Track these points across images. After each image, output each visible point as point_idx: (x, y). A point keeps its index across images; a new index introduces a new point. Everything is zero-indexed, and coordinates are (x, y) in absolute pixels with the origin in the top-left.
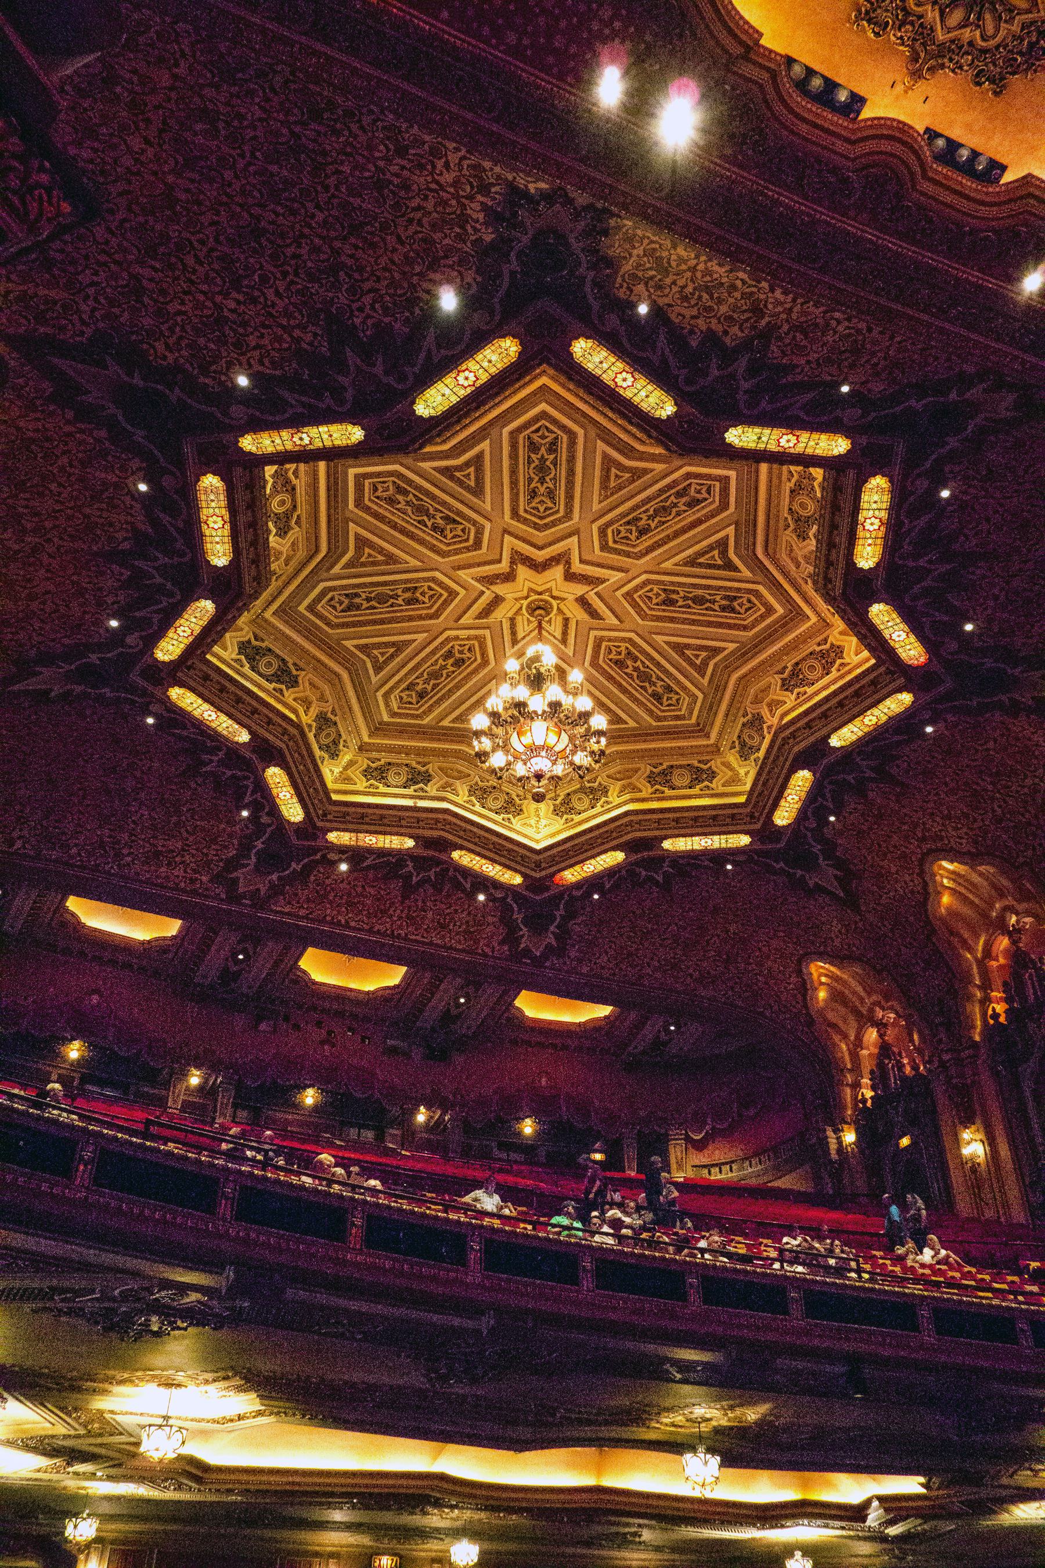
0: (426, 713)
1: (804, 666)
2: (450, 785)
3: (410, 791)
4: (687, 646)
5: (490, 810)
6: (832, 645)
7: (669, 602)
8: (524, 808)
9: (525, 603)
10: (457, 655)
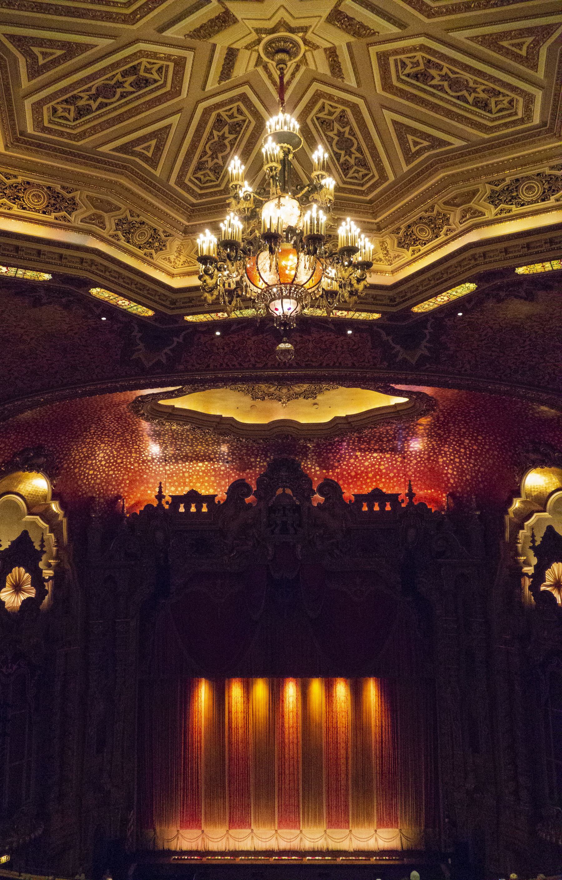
0: (82, 135)
1: (523, 187)
2: (100, 217)
3: (51, 218)
4: (414, 132)
5: (135, 245)
7: (422, 76)
8: (168, 244)
9: (266, 38)
10: (142, 73)
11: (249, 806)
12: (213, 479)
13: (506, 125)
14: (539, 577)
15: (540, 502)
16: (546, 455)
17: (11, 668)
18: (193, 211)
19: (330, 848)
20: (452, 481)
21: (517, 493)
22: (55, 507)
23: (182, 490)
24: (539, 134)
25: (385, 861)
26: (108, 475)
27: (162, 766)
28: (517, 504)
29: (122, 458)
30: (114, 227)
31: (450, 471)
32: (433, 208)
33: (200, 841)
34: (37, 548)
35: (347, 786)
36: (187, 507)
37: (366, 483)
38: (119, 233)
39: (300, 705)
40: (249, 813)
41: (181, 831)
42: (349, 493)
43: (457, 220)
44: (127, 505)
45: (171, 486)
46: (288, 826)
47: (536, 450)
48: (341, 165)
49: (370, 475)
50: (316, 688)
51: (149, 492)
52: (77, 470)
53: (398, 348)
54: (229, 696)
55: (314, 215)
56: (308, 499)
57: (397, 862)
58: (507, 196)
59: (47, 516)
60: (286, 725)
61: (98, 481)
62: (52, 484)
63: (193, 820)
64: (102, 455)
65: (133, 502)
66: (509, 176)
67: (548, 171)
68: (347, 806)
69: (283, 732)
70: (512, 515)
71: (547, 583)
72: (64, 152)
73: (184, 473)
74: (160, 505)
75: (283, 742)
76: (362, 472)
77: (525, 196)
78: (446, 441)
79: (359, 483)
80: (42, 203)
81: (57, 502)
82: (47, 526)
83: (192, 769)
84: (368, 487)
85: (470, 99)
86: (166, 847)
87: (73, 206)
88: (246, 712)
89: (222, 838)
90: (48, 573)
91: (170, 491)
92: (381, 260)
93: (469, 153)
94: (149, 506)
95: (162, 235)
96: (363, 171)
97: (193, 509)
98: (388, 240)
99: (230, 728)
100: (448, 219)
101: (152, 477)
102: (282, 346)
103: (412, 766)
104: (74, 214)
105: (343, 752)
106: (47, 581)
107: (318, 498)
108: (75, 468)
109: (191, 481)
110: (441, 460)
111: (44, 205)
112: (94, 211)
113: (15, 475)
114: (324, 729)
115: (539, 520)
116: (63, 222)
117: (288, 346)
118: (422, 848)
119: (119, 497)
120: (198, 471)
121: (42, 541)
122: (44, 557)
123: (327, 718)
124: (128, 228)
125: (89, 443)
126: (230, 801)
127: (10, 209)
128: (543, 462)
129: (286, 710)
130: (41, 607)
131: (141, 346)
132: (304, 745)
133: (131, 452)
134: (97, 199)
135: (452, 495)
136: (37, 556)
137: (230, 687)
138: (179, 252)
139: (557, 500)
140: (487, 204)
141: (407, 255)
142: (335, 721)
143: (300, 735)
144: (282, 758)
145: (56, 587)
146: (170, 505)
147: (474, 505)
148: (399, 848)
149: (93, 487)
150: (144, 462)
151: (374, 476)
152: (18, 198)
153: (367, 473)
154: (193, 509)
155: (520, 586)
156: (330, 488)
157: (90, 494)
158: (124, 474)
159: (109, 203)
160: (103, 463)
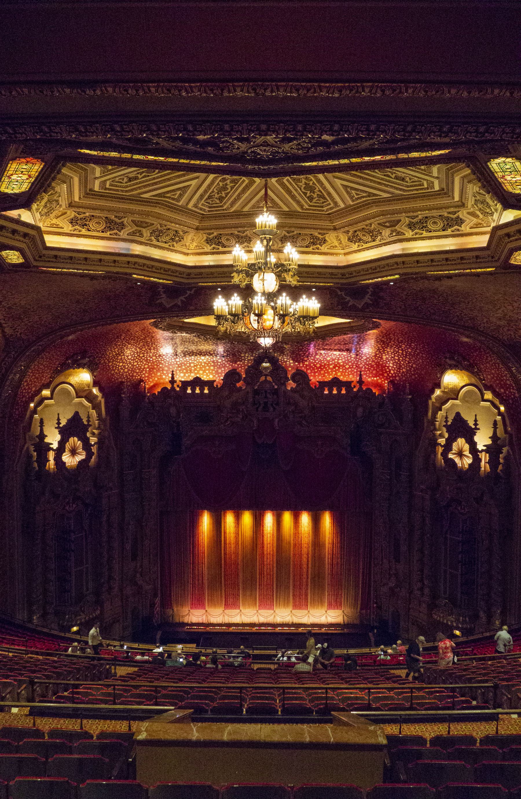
3: (107, 234)
5: (162, 242)
6: (458, 217)
11: (238, 595)
12: (212, 368)
13: (417, 190)
14: (448, 447)
15: (453, 393)
16: (458, 362)
18: (203, 218)
19: (294, 622)
20: (392, 372)
21: (438, 385)
22: (95, 391)
23: (189, 376)
24: (439, 194)
25: (332, 630)
26: (133, 365)
27: (175, 566)
28: (438, 392)
29: (143, 353)
30: (149, 235)
31: (391, 365)
32: (371, 224)
33: (204, 617)
34: (86, 423)
35: (307, 582)
36: (193, 390)
37: (328, 373)
38: (153, 238)
39: (275, 529)
40: (238, 599)
41: (191, 611)
42: (314, 379)
43: (387, 234)
44: (147, 386)
45: (180, 373)
46: (265, 608)
47: (452, 358)
48: (308, 198)
49: (331, 367)
50: (287, 517)
51: (164, 377)
52: (110, 364)
53: (348, 298)
54: (225, 522)
55: (284, 302)
56: (284, 384)
57: (339, 632)
58: (420, 225)
59: (90, 397)
60: (265, 542)
61: (126, 370)
62: (93, 375)
63: (199, 603)
64: (129, 352)
65: (152, 384)
66: (421, 215)
67: (446, 214)
68: (306, 595)
69: (263, 547)
70: (434, 400)
71: (453, 452)
72: (117, 198)
73: (190, 363)
74: (173, 388)
75: (263, 553)
76: (325, 365)
77: (430, 226)
78: (388, 345)
79: (322, 372)
80: (102, 226)
81: (97, 388)
82: (90, 405)
83: (198, 570)
84: (329, 374)
85: (393, 176)
86: (181, 620)
87: (122, 226)
88: (237, 533)
89: (220, 615)
90: (93, 440)
91: (180, 377)
92: (336, 247)
93: (394, 200)
94: (165, 388)
95: (181, 233)
96: (322, 200)
97: (198, 391)
98: (341, 236)
99: (225, 543)
100: (381, 233)
101: (166, 366)
102: (264, 365)
103: (355, 566)
104: (122, 231)
105: (305, 560)
106: (93, 446)
107: (291, 385)
108: (109, 362)
109: (195, 370)
110: (384, 357)
111: (103, 228)
112: (136, 228)
113: (67, 372)
114: (292, 545)
115: (453, 405)
116: (115, 236)
117: (268, 365)
118: (357, 622)
119: (141, 381)
120: (201, 363)
121: (88, 417)
122: (90, 429)
123: (295, 537)
124: (158, 234)
125: (119, 345)
126: (225, 592)
127: (80, 231)
128: (456, 366)
129: (265, 532)
130: (90, 464)
131: (164, 296)
132: (277, 556)
133: (150, 349)
134: (138, 221)
135: (392, 382)
136: (85, 428)
137: (225, 516)
138: (193, 240)
139: (466, 392)
140: (406, 228)
141: (355, 247)
142: (299, 540)
143: (275, 549)
144: (262, 563)
145: (99, 449)
146: (180, 388)
147: (408, 391)
148: (342, 622)
149: (123, 375)
150: (160, 356)
151: (334, 367)
152: (86, 225)
153: (329, 365)
154: (198, 391)
155: (435, 453)
156: (301, 377)
157: (120, 380)
158: (145, 364)
159: (147, 223)
160: (130, 357)
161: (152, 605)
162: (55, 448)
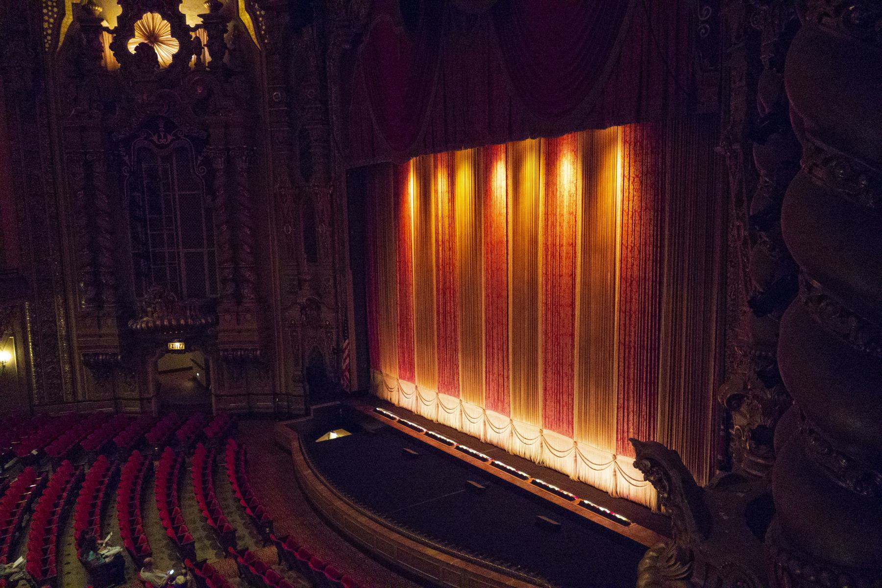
17: (165, 137)
54: (436, 191)
161: (338, 351)
162: (112, 28)
